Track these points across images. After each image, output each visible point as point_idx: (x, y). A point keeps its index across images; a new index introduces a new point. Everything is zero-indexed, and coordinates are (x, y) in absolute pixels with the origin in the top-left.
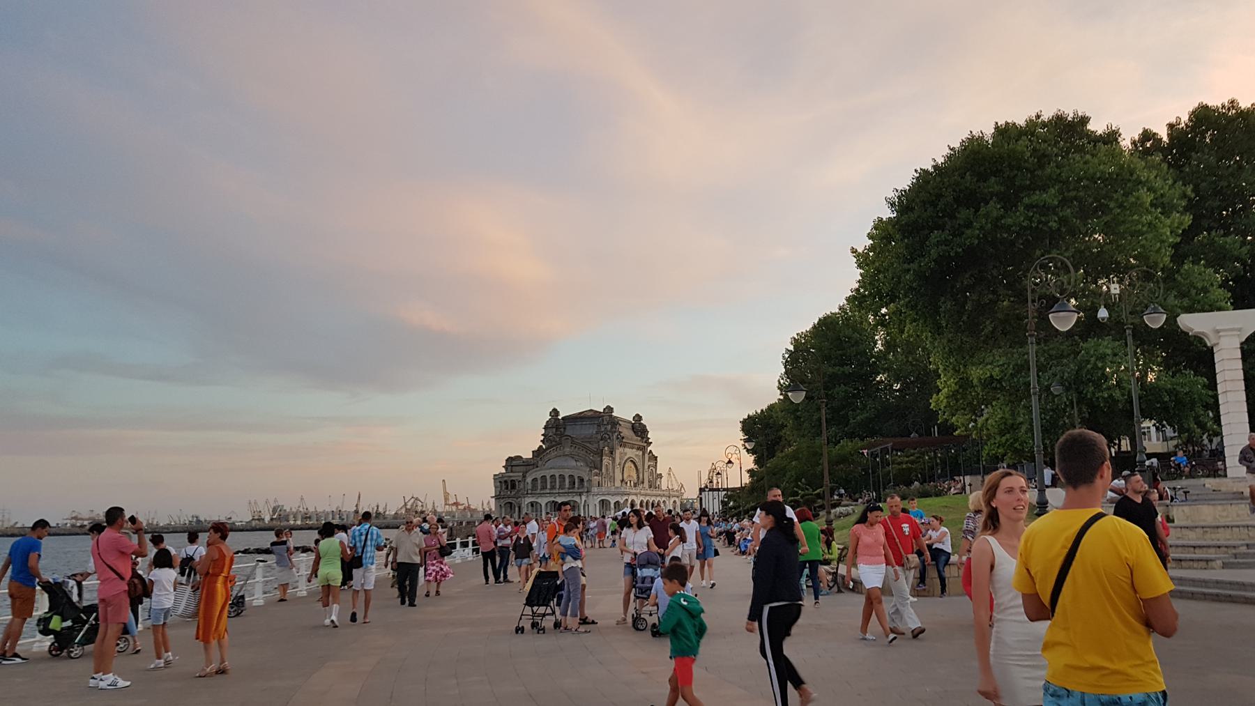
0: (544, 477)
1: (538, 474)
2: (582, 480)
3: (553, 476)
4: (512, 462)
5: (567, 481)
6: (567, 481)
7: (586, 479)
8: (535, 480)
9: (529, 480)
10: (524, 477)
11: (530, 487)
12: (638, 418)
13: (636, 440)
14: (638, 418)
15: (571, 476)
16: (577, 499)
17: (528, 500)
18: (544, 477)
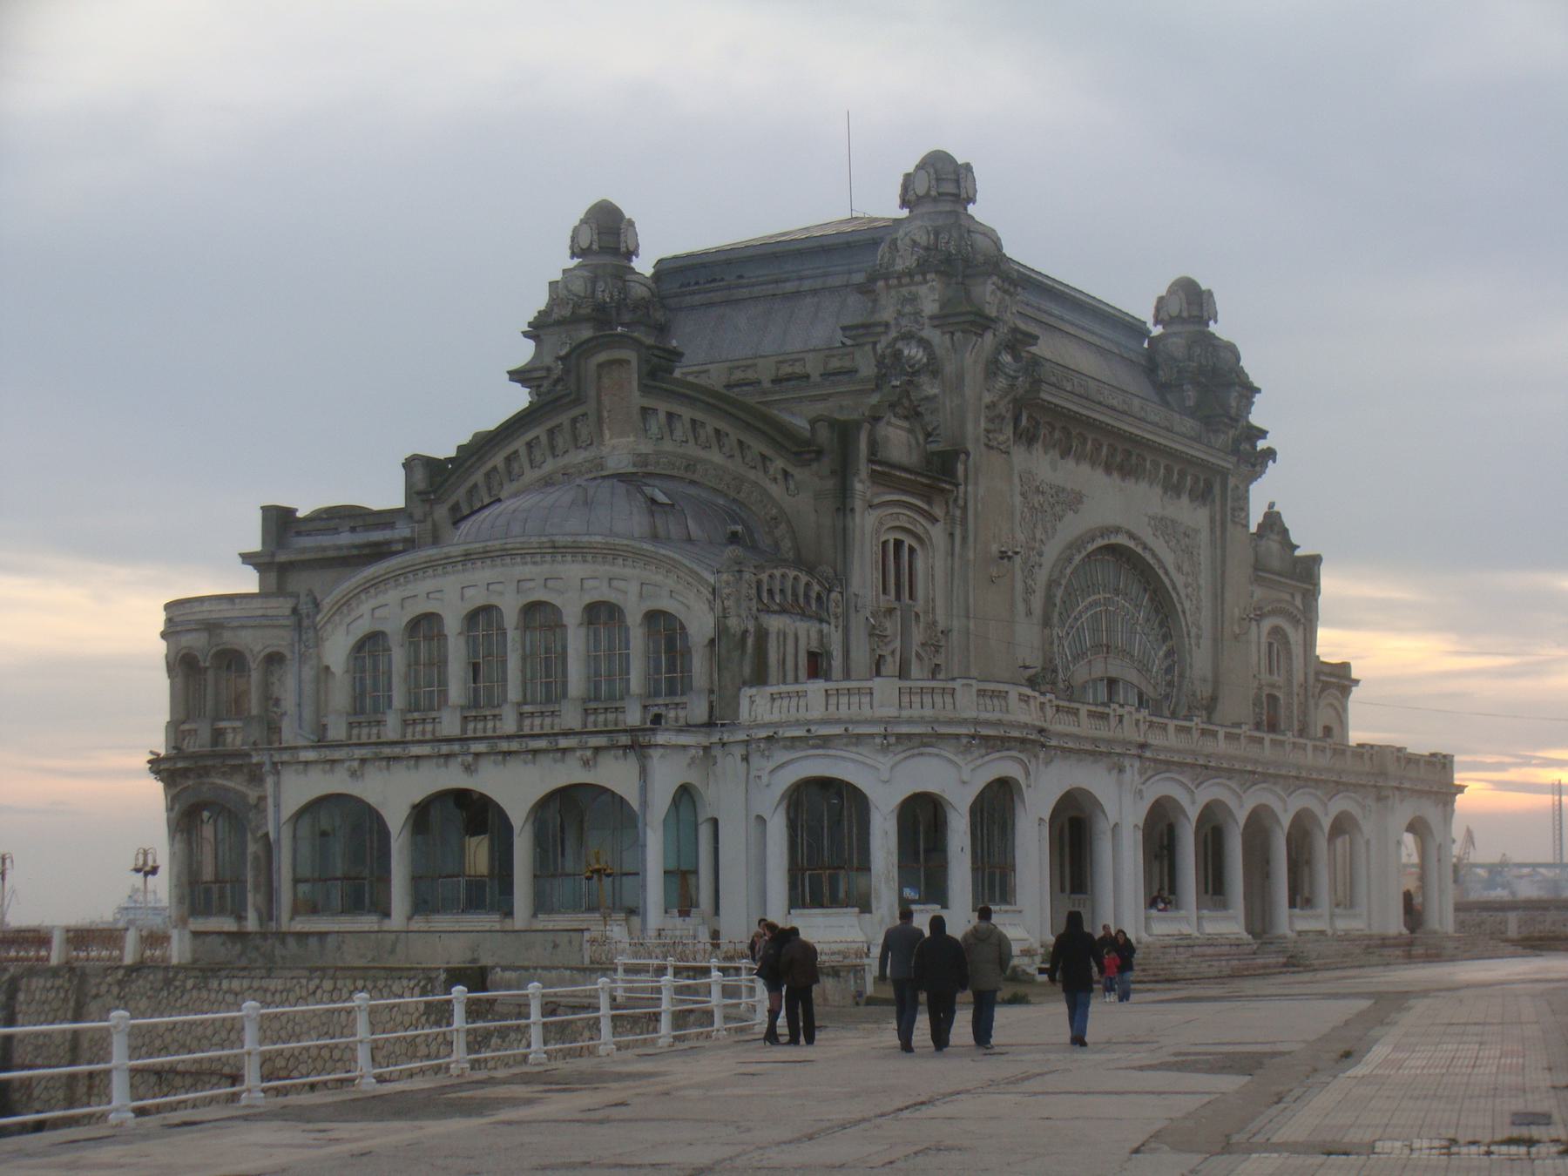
0: (425, 626)
1: (388, 608)
2: (663, 625)
3: (481, 617)
4: (297, 547)
5: (576, 641)
6: (576, 641)
7: (699, 624)
8: (371, 643)
9: (337, 649)
10: (304, 623)
11: (340, 696)
12: (1190, 303)
13: (1175, 429)
14: (1190, 303)
15: (601, 614)
16: (616, 775)
17: (297, 789)
18: (425, 626)
